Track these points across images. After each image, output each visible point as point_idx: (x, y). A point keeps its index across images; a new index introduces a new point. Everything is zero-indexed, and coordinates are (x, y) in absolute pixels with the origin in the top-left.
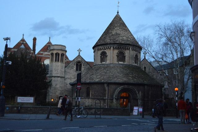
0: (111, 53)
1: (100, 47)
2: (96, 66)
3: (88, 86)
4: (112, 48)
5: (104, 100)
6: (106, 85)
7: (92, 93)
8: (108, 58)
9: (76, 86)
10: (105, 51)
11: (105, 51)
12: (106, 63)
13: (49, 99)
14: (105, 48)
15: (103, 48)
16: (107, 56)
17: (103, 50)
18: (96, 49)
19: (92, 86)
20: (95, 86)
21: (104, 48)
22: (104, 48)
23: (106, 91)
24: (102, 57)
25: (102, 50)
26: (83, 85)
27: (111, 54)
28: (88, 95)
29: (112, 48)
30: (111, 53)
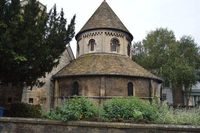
0: (124, 42)
1: (110, 32)
2: (105, 54)
3: (129, 81)
4: (125, 37)
5: (151, 100)
6: (152, 81)
7: (136, 91)
8: (121, 47)
9: (103, 79)
10: (117, 38)
11: (117, 38)
12: (119, 54)
13: (26, 100)
14: (119, 35)
15: (116, 35)
16: (119, 45)
17: (114, 37)
18: (104, 32)
19: (136, 81)
20: (140, 82)
21: (117, 34)
22: (117, 34)
23: (152, 89)
24: (112, 44)
25: (113, 35)
26: (121, 79)
27: (124, 44)
28: (130, 93)
29: (125, 37)
30: (124, 42)
